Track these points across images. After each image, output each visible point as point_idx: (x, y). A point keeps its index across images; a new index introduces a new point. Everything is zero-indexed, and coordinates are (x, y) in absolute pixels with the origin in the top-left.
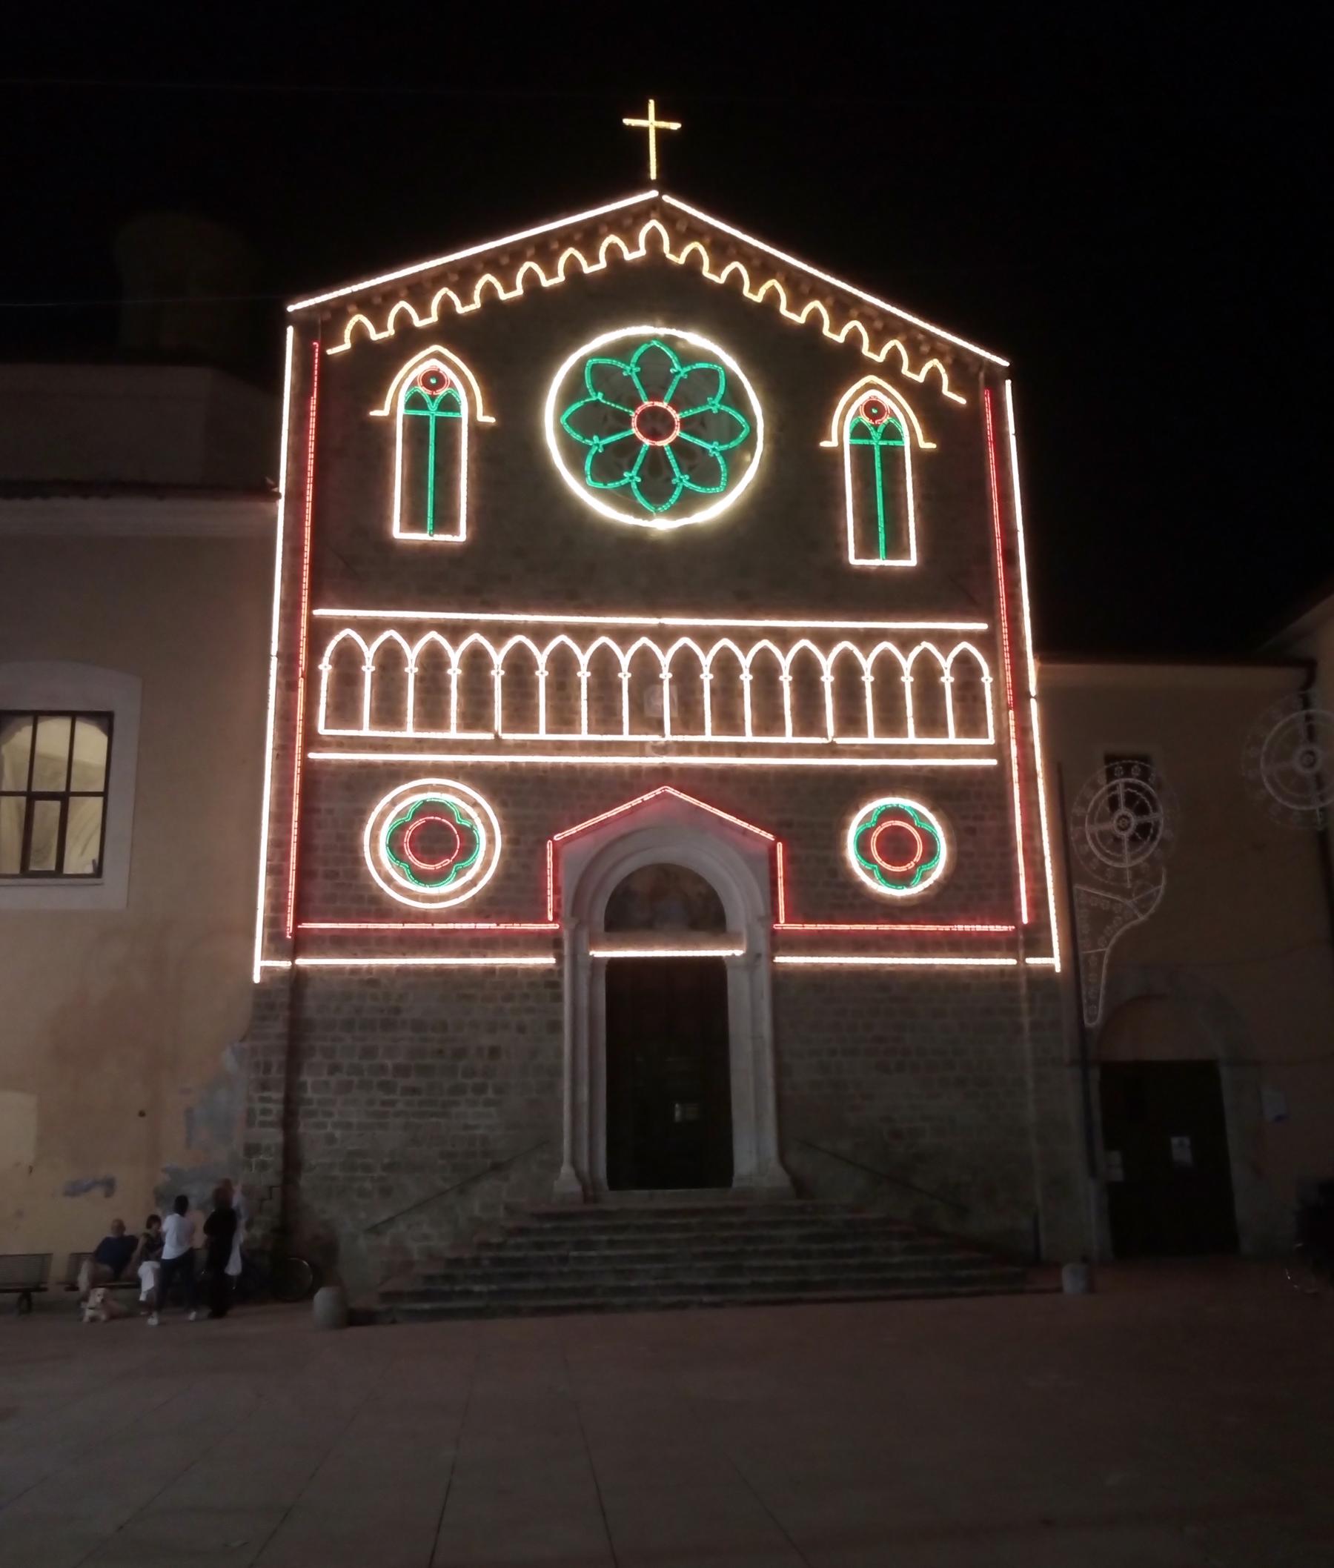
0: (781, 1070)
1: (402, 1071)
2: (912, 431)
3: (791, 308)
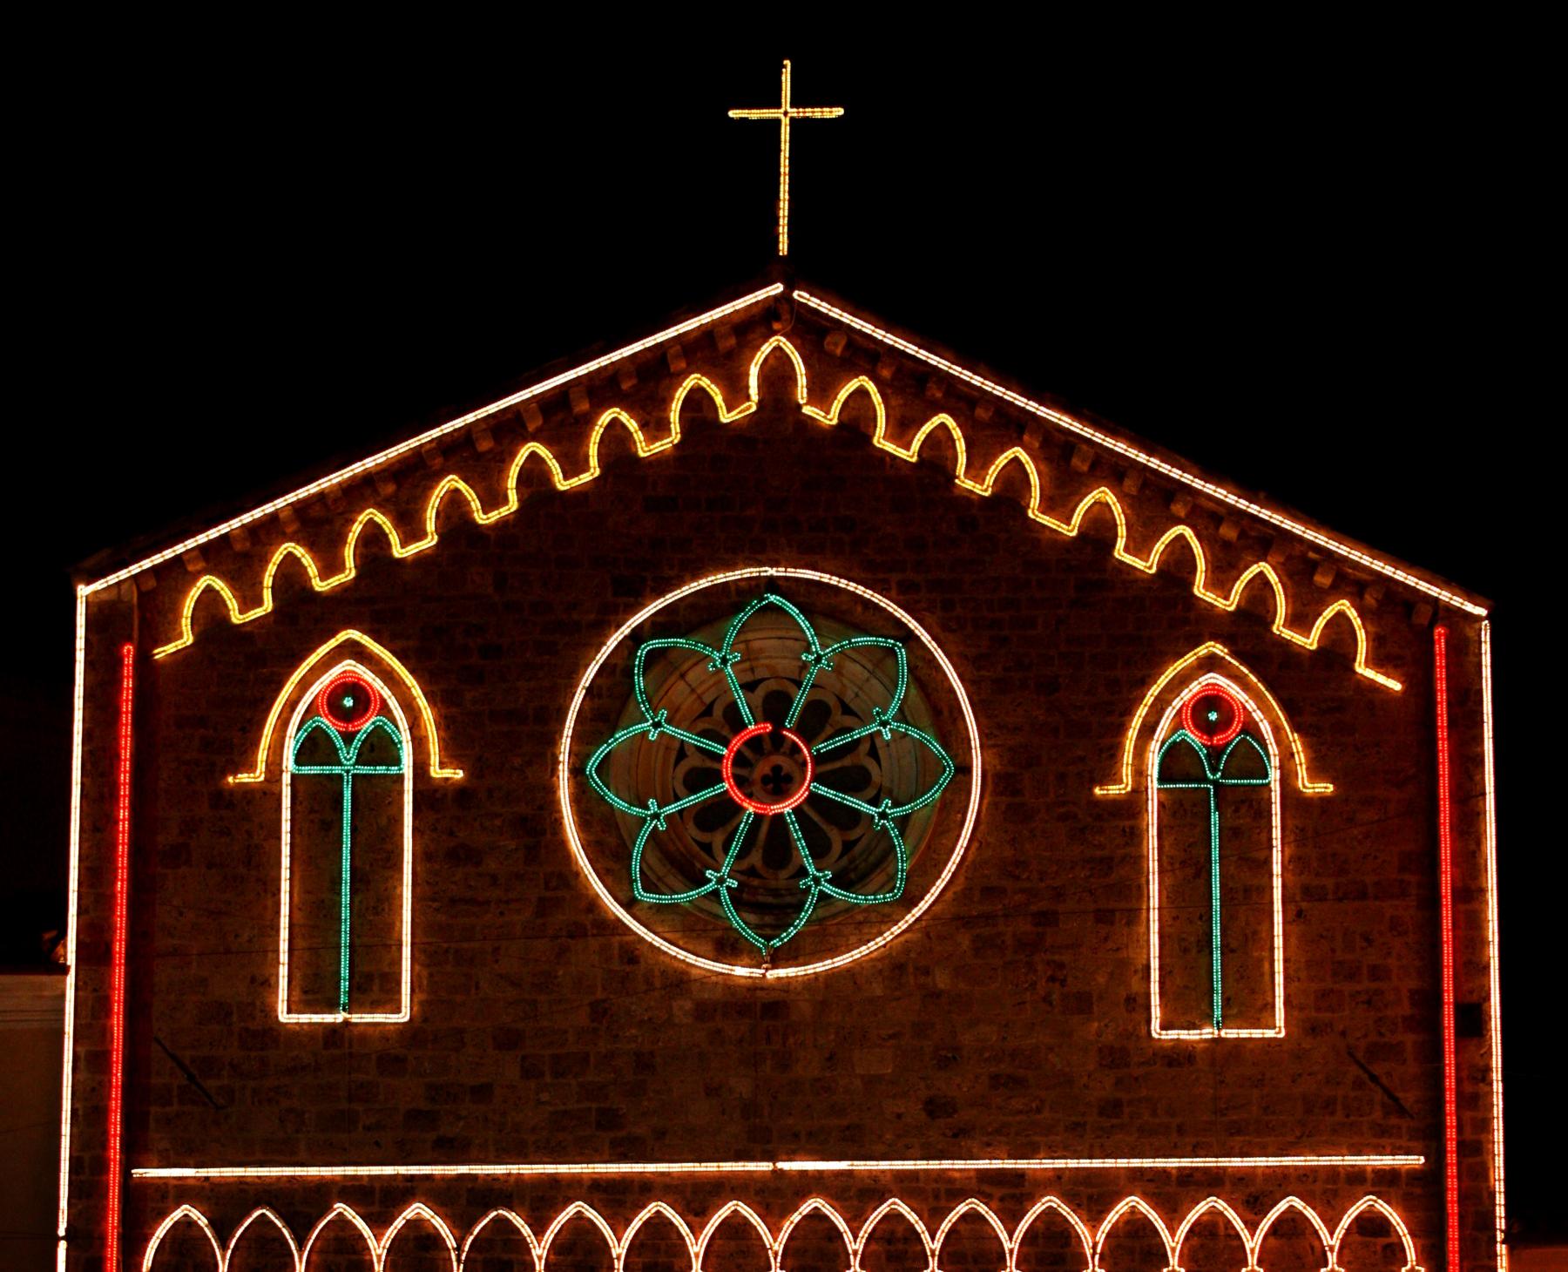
2: (1287, 756)
3: (1048, 506)
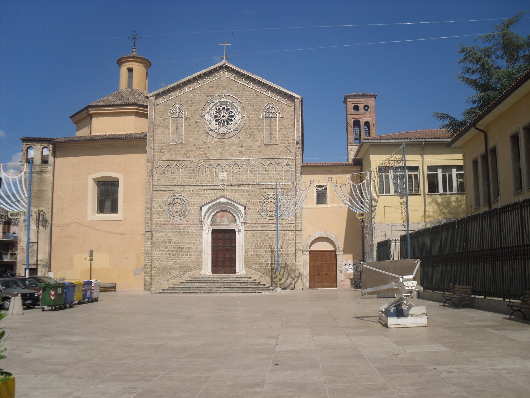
0: (246, 252)
1: (172, 251)
